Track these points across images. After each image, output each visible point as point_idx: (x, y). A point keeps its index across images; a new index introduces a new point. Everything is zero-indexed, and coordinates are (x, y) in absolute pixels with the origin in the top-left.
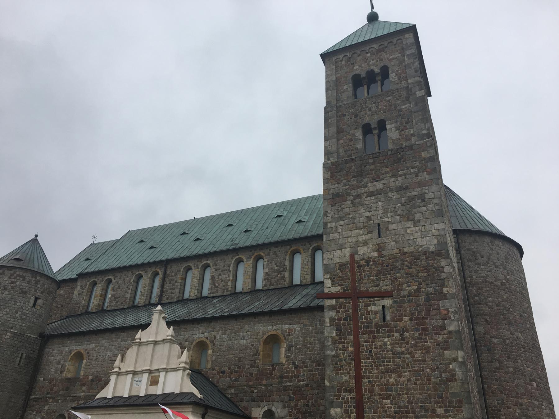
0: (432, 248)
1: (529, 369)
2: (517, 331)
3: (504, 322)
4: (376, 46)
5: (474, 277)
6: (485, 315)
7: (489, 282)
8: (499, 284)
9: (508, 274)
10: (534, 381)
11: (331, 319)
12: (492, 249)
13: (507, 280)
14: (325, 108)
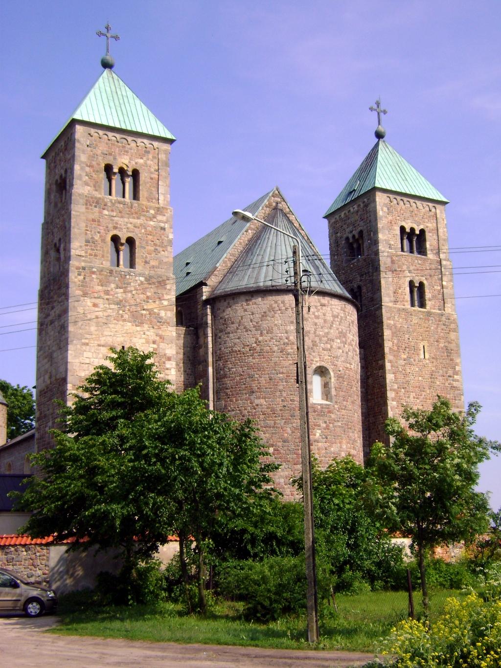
0: (64, 376)
1: (267, 435)
2: (259, 398)
3: (244, 392)
4: (62, 143)
5: (223, 349)
6: (227, 389)
7: (236, 352)
8: (248, 350)
9: (261, 335)
10: (272, 446)
11: (38, 439)
12: (245, 310)
13: (257, 342)
14: (43, 225)
